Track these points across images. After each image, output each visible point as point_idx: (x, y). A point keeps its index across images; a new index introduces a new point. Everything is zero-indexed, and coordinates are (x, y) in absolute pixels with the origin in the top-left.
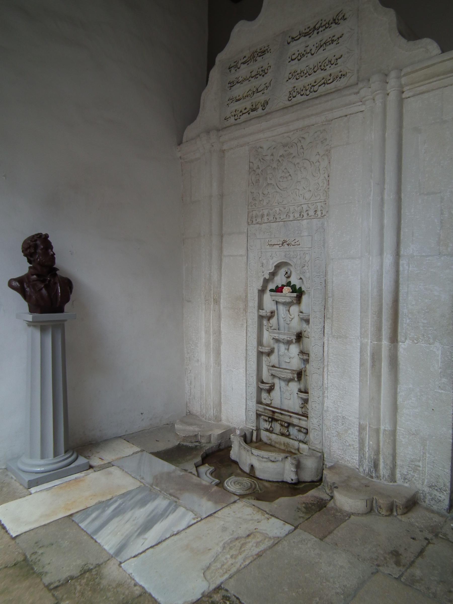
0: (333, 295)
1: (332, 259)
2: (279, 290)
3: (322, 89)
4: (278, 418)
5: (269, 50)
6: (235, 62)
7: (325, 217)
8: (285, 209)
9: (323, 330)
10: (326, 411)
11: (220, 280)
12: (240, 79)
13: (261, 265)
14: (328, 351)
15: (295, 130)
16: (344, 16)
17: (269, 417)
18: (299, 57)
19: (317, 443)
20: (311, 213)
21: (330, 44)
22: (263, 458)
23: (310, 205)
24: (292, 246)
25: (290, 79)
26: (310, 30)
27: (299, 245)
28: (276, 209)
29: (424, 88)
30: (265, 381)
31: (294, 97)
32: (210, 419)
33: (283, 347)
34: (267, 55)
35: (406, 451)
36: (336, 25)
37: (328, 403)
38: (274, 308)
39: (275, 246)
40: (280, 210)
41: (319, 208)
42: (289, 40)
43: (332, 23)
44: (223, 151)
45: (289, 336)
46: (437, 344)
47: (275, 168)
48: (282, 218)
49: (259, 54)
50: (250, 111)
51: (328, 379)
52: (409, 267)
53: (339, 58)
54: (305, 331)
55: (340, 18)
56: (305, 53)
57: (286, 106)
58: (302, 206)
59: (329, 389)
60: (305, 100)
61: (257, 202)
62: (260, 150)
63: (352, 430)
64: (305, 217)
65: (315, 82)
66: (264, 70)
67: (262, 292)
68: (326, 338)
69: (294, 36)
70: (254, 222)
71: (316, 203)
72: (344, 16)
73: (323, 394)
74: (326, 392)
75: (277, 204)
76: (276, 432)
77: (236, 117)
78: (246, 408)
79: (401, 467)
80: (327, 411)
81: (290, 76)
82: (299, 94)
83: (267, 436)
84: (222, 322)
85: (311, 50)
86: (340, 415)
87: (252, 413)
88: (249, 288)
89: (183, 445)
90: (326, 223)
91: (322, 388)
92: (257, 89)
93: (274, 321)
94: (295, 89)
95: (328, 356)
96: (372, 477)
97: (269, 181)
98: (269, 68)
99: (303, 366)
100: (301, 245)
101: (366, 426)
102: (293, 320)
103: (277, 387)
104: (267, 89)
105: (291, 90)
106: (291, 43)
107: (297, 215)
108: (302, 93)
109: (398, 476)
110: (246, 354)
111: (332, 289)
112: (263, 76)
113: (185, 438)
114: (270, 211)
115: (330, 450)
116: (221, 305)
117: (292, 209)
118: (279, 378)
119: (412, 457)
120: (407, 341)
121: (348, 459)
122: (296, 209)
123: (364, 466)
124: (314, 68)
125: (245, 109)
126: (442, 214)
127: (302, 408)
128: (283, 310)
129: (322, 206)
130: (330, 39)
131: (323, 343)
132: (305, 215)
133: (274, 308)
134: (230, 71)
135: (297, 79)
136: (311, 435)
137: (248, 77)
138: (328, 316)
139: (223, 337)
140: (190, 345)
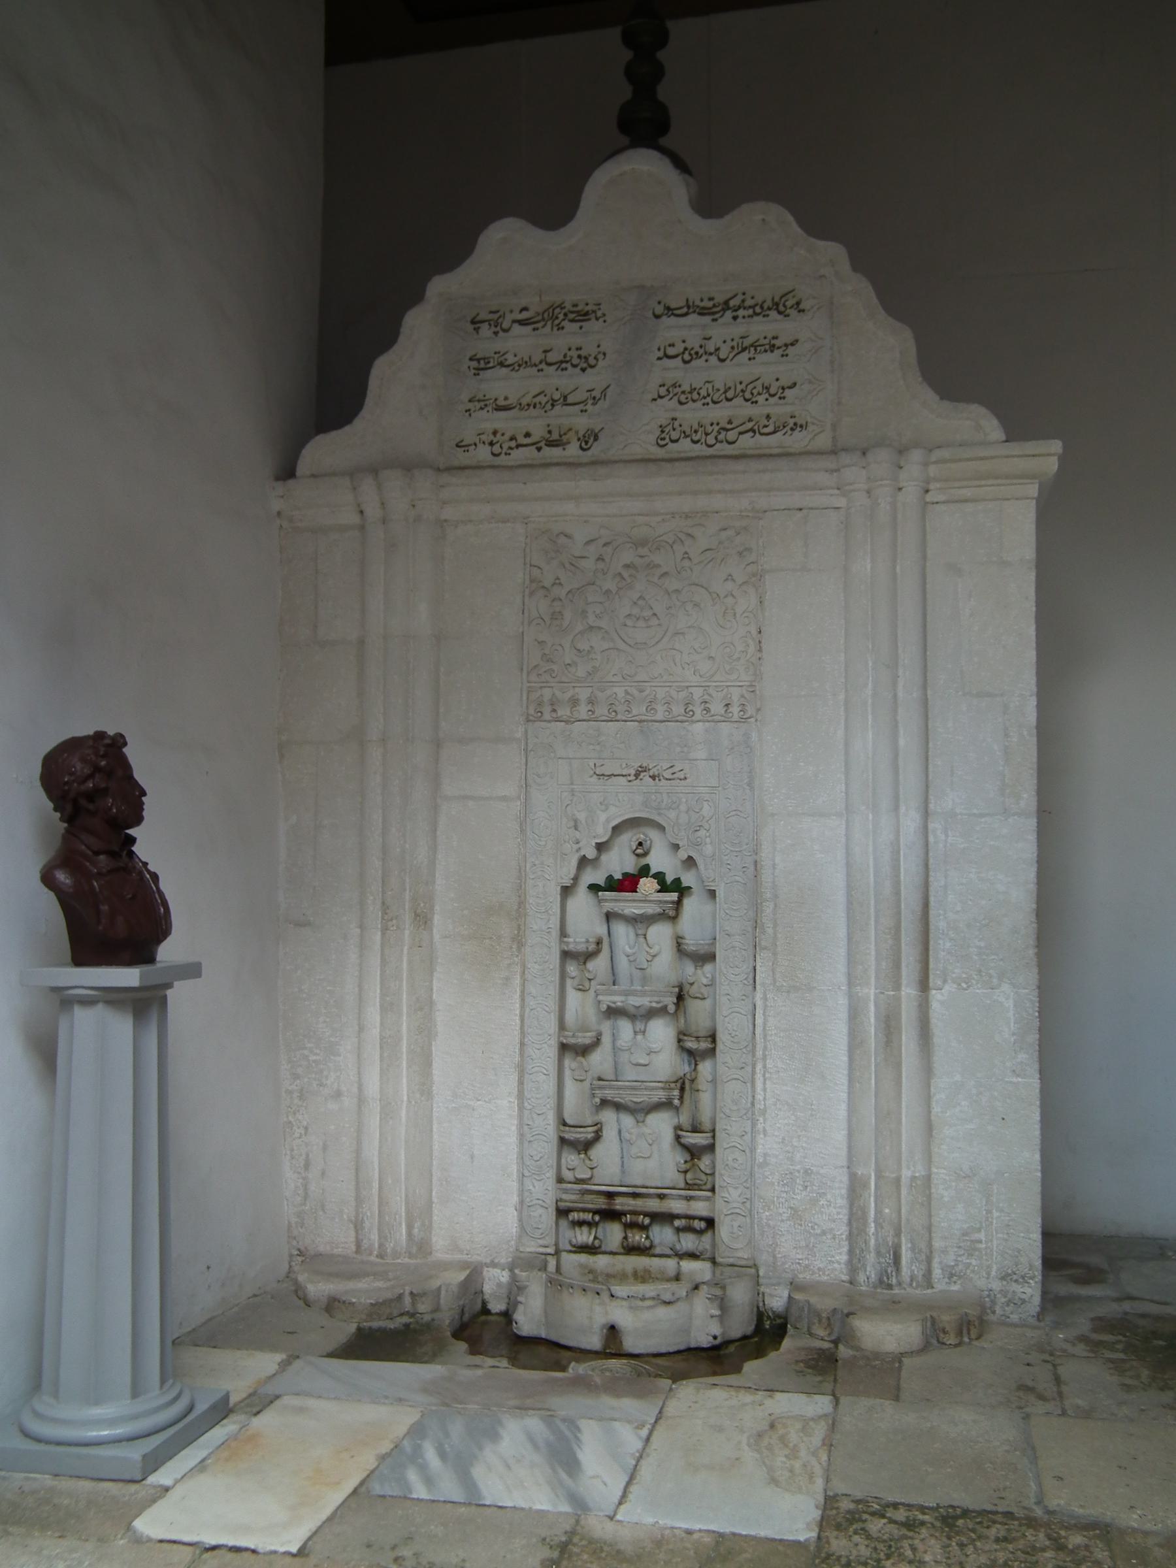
0: (776, 896)
1: (773, 815)
2: (628, 883)
3: (746, 442)
4: (626, 1208)
5: (599, 314)
6: (491, 312)
7: (752, 720)
8: (641, 691)
9: (751, 976)
10: (761, 1166)
11: (432, 863)
12: (511, 359)
13: (572, 824)
14: (765, 1024)
15: (667, 514)
16: (798, 304)
17: (595, 1212)
18: (687, 357)
20: (717, 708)
21: (766, 351)
22: (643, 1299)
23: (711, 691)
25: (661, 397)
26: (714, 306)
28: (616, 690)
29: (967, 493)
30: (569, 1121)
31: (673, 441)
32: (396, 1254)
34: (592, 325)
35: (952, 1217)
36: (780, 317)
37: (767, 1145)
38: (601, 930)
40: (627, 693)
41: (735, 698)
42: (659, 310)
43: (769, 309)
44: (442, 523)
45: (656, 999)
46: (1006, 987)
47: (608, 592)
48: (635, 712)
49: (572, 316)
50: (542, 444)
51: (765, 1090)
52: (947, 836)
53: (790, 388)
54: (692, 984)
55: (789, 304)
56: (701, 351)
57: (652, 457)
58: (691, 690)
60: (704, 454)
61: (554, 667)
62: (562, 540)
63: (829, 1197)
64: (698, 716)
65: (730, 422)
66: (586, 358)
67: (567, 891)
69: (673, 306)
70: (547, 716)
72: (798, 304)
73: (754, 1125)
74: (761, 1120)
76: (608, 1249)
77: (496, 449)
79: (943, 1252)
80: (765, 1164)
81: (663, 391)
82: (686, 437)
83: (582, 1266)
85: (717, 349)
86: (798, 1167)
87: (541, 1211)
89: (370, 1328)
92: (565, 398)
93: (599, 965)
94: (676, 424)
95: (765, 1036)
96: (890, 1287)
97: (591, 620)
98: (601, 357)
99: (687, 1069)
101: (870, 1178)
102: (656, 959)
103: (610, 1133)
104: (594, 404)
105: (664, 423)
106: (664, 318)
107: (678, 710)
108: (695, 438)
109: (937, 1272)
110: (522, 1054)
111: (774, 882)
112: (583, 370)
113: (376, 1308)
114: (599, 694)
115: (774, 1257)
116: (435, 931)
117: (661, 693)
118: (619, 1107)
119: (965, 1226)
120: (947, 987)
121: (821, 1266)
122: (674, 694)
123: (868, 1269)
124: (725, 392)
125: (527, 435)
126: (1006, 735)
127: (686, 1172)
128: (627, 935)
129: (742, 696)
130: (767, 341)
131: (751, 1007)
132: (698, 711)
134: (477, 330)
135: (681, 403)
136: (724, 1230)
137: (536, 359)
138: (763, 943)
139: (440, 1018)
140: (306, 1052)
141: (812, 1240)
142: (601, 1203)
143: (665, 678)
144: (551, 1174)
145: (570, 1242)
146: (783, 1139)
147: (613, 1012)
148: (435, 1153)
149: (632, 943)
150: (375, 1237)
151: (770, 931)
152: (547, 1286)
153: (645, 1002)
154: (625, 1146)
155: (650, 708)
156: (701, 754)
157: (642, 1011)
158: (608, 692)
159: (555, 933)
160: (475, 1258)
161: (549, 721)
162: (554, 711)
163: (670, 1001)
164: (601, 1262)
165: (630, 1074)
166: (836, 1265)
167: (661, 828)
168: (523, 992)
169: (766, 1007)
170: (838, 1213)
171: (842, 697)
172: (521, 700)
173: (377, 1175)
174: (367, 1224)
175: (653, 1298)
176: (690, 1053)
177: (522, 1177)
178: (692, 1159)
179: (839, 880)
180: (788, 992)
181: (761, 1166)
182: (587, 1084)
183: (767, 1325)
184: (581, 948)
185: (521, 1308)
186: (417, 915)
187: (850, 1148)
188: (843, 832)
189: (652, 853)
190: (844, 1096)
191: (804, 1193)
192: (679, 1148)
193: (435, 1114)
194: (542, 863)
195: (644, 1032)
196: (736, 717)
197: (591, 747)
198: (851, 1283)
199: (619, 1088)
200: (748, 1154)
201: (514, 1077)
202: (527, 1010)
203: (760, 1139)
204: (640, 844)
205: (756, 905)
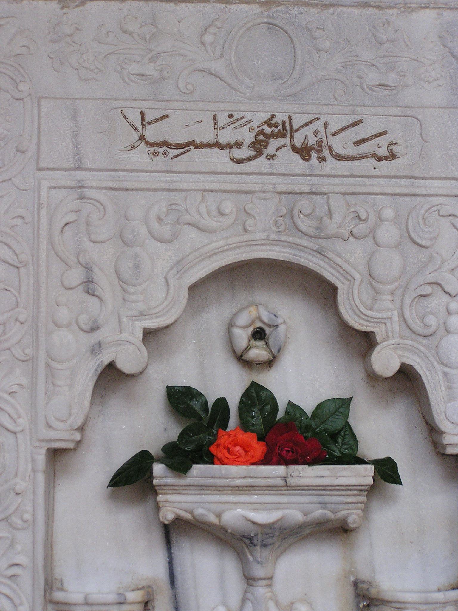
13: (76, 276)
24: (332, 165)
27: (392, 156)
167: (323, 292)
204: (259, 334)
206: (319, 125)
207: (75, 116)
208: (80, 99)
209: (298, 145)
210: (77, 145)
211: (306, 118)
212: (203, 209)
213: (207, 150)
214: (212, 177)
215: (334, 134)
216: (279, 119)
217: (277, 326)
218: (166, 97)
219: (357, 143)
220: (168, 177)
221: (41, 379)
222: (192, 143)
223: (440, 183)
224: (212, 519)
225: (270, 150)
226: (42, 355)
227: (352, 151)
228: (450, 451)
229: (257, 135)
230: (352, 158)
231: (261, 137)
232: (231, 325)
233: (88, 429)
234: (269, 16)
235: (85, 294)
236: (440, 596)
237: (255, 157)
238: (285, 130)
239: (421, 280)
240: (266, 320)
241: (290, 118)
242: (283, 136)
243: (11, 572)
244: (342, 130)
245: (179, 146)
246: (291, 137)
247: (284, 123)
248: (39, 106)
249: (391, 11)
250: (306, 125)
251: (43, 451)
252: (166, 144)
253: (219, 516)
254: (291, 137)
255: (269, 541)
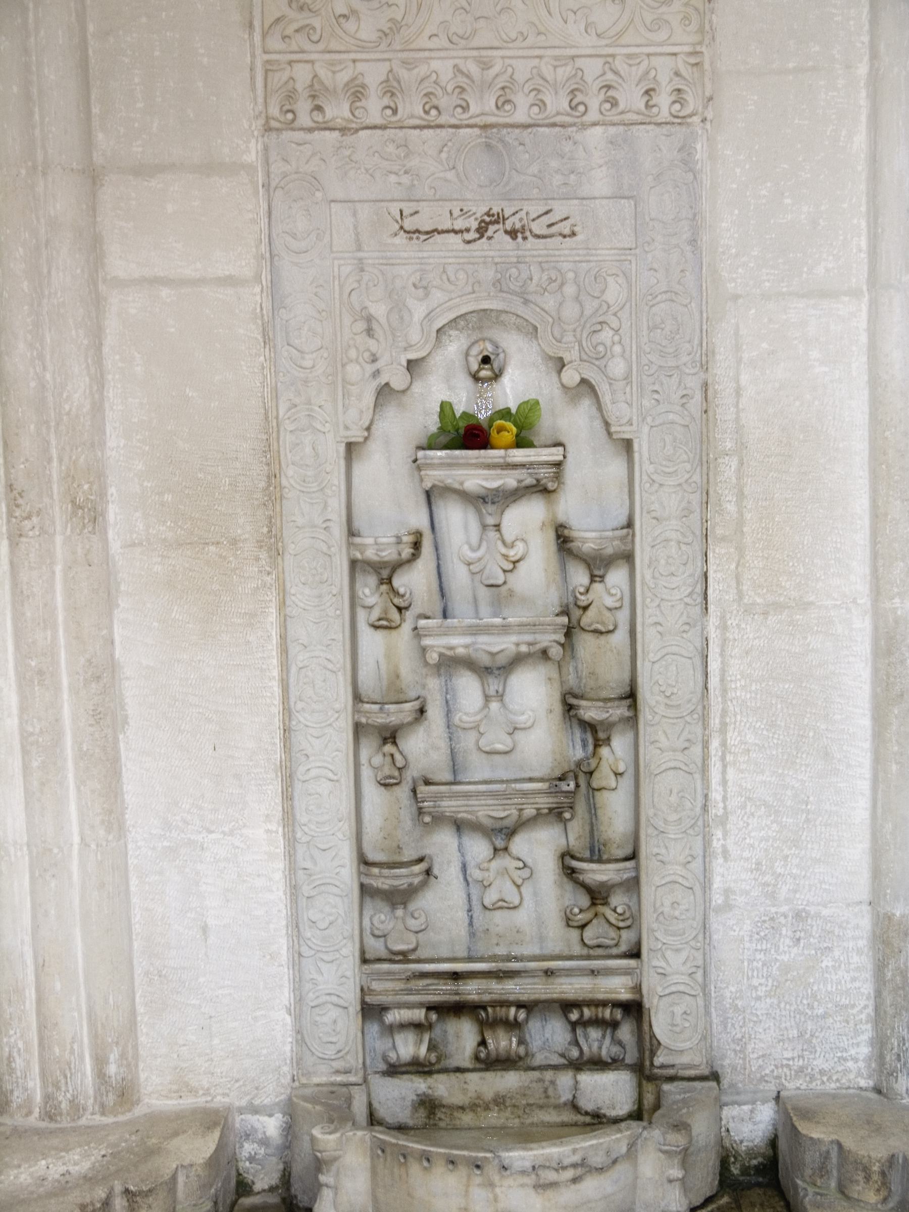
1: (736, 297)
4: (486, 998)
7: (696, 119)
9: (699, 589)
11: (98, 409)
13: (361, 326)
17: (430, 1008)
19: (688, 1045)
20: (631, 98)
23: (619, 64)
27: (574, 234)
28: (435, 65)
33: (469, 690)
39: (438, 238)
45: (528, 638)
51: (724, 782)
54: (585, 608)
58: (580, 63)
59: (732, 818)
61: (317, 22)
63: (837, 953)
64: (593, 115)
68: (713, 620)
70: (304, 119)
71: (648, 55)
74: (719, 833)
75: (443, 42)
78: (300, 1000)
84: (118, 614)
86: (785, 909)
87: (334, 1013)
88: (288, 439)
90: (699, 147)
91: (703, 821)
93: (416, 581)
95: (724, 691)
100: (579, 237)
107: (557, 103)
111: (737, 419)
118: (459, 826)
121: (826, 1066)
127: (583, 927)
128: (466, 527)
129: (677, 74)
132: (594, 103)
133: (419, 519)
138: (719, 531)
139: (133, 692)
141: (810, 1026)
142: (443, 992)
143: (530, 41)
144: (350, 951)
145: (385, 1058)
146: (758, 864)
147: (450, 664)
148: (137, 928)
149: (475, 540)
150: (35, 1085)
151: (731, 508)
152: (374, 1157)
153: (506, 644)
154: (475, 891)
155: (503, 103)
156: (600, 182)
157: (502, 660)
158: (423, 70)
159: (338, 531)
160: (220, 1101)
161: (310, 130)
162: (319, 108)
163: (550, 639)
164: (442, 1087)
165: (479, 769)
166: (850, 1064)
168: (283, 638)
169: (724, 641)
170: (854, 980)
171: (863, 70)
172: (253, 88)
173: (31, 978)
174: (19, 1063)
175: (574, 1166)
176: (590, 727)
177: (297, 958)
178: (593, 904)
179: (856, 410)
180: (765, 613)
181: (719, 910)
182: (403, 792)
183: (735, 1170)
184: (389, 554)
185: (327, 1195)
186: (76, 506)
187: (877, 873)
188: (864, 324)
189: (506, 379)
190: (865, 786)
191: (795, 950)
192: (569, 886)
193: (132, 861)
194: (309, 403)
195: (500, 696)
196: (664, 115)
197: (393, 178)
198: (878, 1091)
199: (467, 795)
200: (697, 888)
201: (274, 788)
202: (293, 670)
203: (718, 865)
204: (486, 360)
205: (706, 463)
206: (522, 214)
207: (355, 214)
208: (360, 201)
209: (509, 229)
210: (357, 234)
211: (513, 210)
212: (444, 277)
213: (446, 235)
214: (450, 254)
215: (533, 220)
216: (495, 210)
217: (498, 355)
218: (417, 198)
219: (550, 226)
220: (420, 255)
221: (340, 397)
222: (435, 230)
223: (607, 252)
224: (456, 486)
225: (490, 233)
226: (340, 378)
227: (545, 231)
228: (615, 437)
229: (480, 223)
230: (544, 237)
231: (483, 224)
232: (467, 354)
233: (374, 427)
234: (486, 137)
235: (367, 338)
236: (610, 534)
237: (479, 239)
238: (499, 219)
239: (594, 321)
240: (490, 350)
241: (502, 210)
242: (498, 223)
243: (324, 526)
244: (539, 217)
245: (427, 233)
246: (504, 223)
247: (498, 214)
248: (330, 209)
249: (570, 129)
250: (514, 214)
251: (344, 445)
252: (418, 231)
253: (462, 484)
254: (504, 223)
255: (496, 500)
